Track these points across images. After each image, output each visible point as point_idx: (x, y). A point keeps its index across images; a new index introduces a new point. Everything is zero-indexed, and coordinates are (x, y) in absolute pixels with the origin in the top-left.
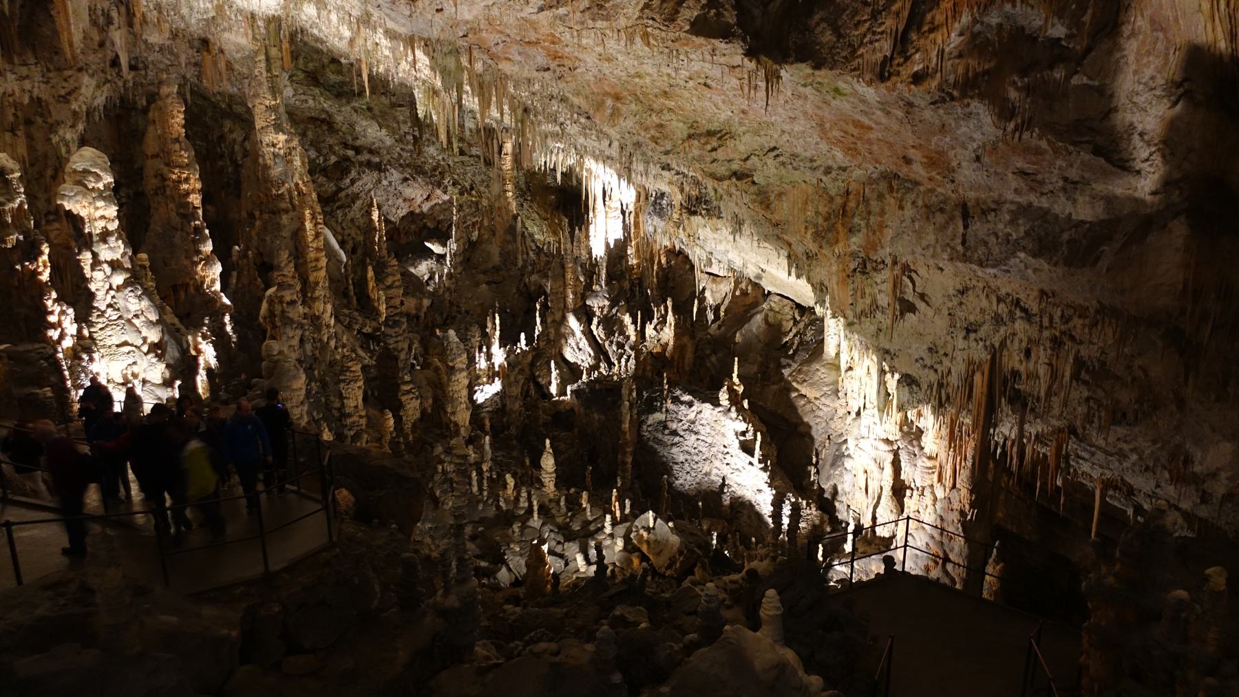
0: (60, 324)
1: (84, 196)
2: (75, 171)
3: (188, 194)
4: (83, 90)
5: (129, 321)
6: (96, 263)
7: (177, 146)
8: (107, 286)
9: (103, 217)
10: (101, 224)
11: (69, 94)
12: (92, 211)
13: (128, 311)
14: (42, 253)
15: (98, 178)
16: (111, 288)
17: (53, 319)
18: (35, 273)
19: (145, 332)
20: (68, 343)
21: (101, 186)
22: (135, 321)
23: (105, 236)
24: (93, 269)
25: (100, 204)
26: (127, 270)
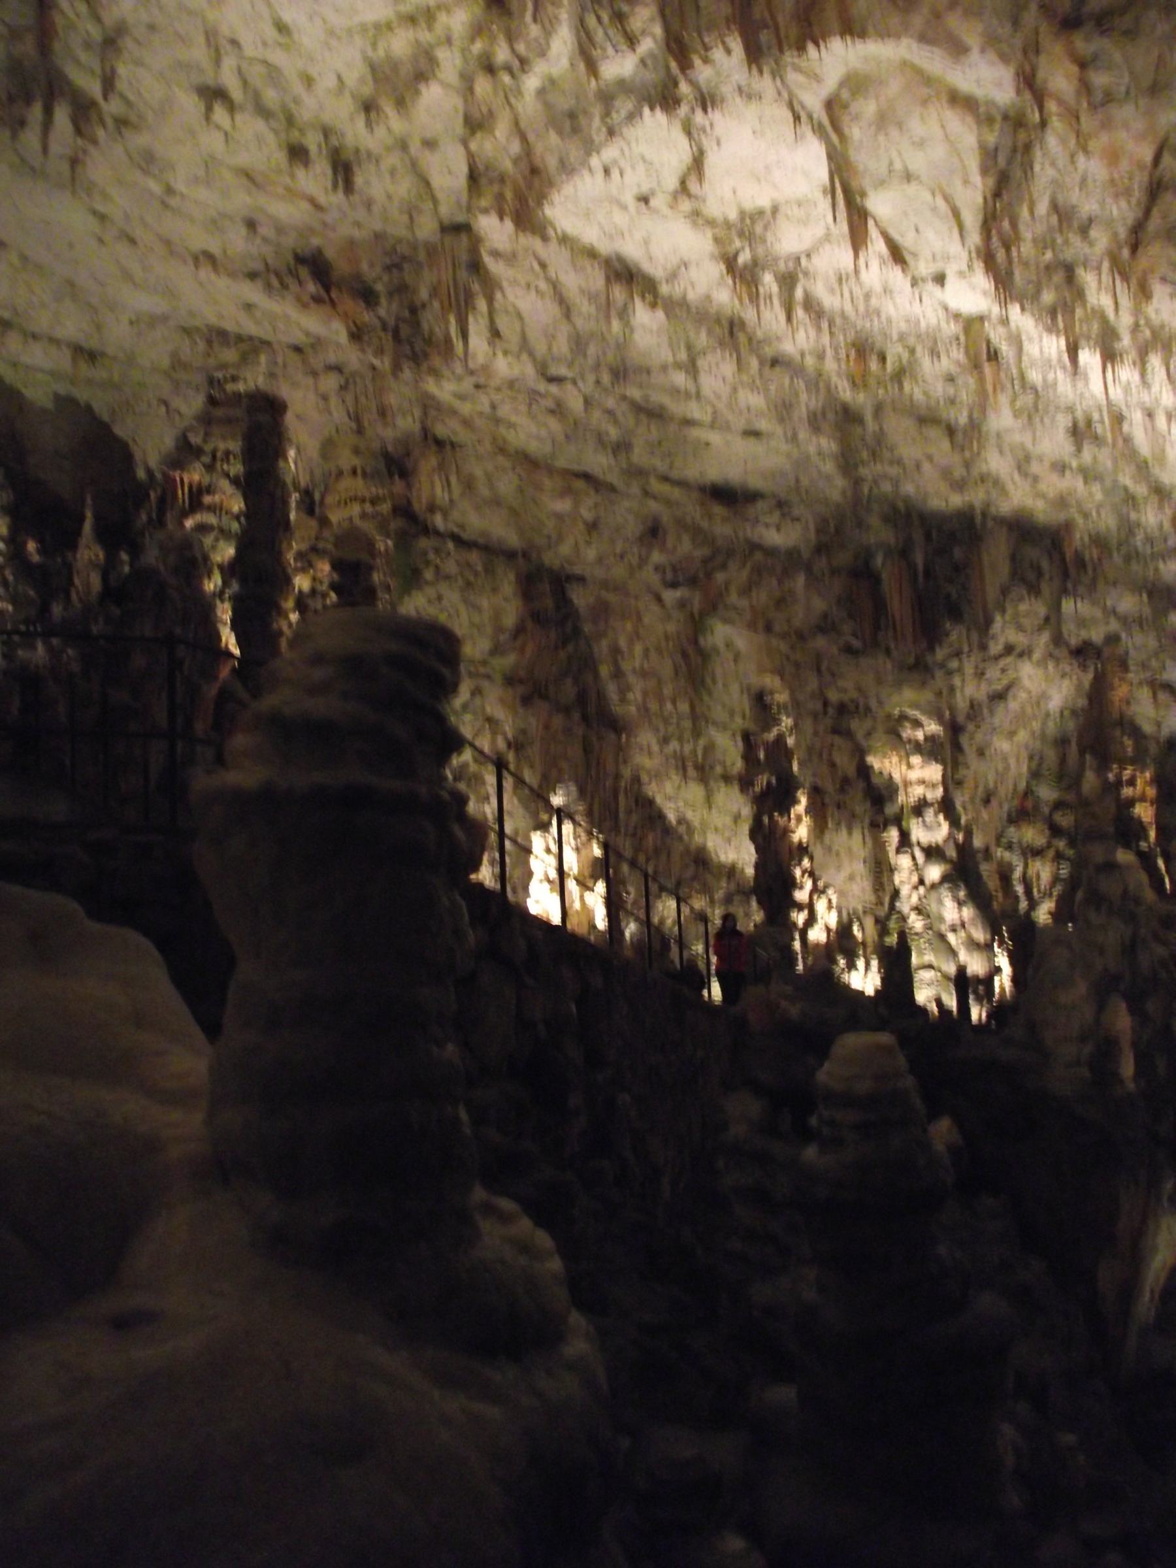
0: (811, 907)
1: (894, 748)
2: (889, 716)
3: (1131, 803)
4: (1026, 682)
5: (942, 937)
6: (905, 841)
7: (1118, 733)
8: (915, 879)
9: (922, 782)
10: (918, 791)
11: (1008, 688)
12: (904, 767)
13: (941, 919)
14: (796, 801)
15: (917, 724)
16: (921, 882)
17: (801, 896)
18: (787, 831)
19: (963, 956)
20: (817, 935)
21: (920, 735)
22: (952, 938)
23: (919, 809)
24: (898, 851)
25: (916, 760)
26: (951, 861)
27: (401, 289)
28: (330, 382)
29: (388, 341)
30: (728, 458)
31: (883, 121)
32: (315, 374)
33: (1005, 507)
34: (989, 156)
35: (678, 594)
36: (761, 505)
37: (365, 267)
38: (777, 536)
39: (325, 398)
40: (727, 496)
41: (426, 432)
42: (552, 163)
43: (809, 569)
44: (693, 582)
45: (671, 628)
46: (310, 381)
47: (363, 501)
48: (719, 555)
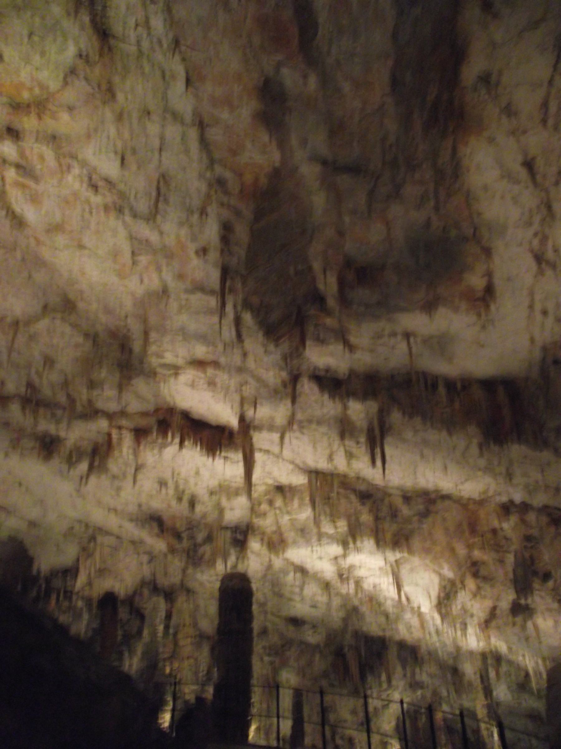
27: (192, 537)
28: (145, 558)
29: (184, 555)
30: (300, 609)
31: (412, 570)
32: (138, 554)
33: (397, 638)
34: (443, 588)
35: (270, 659)
36: (306, 626)
37: (178, 525)
38: (312, 638)
39: (142, 564)
40: (296, 622)
41: (182, 584)
42: (290, 540)
43: (321, 652)
44: (277, 654)
45: (265, 672)
46: (136, 556)
47: (192, 637)
48: (287, 644)
